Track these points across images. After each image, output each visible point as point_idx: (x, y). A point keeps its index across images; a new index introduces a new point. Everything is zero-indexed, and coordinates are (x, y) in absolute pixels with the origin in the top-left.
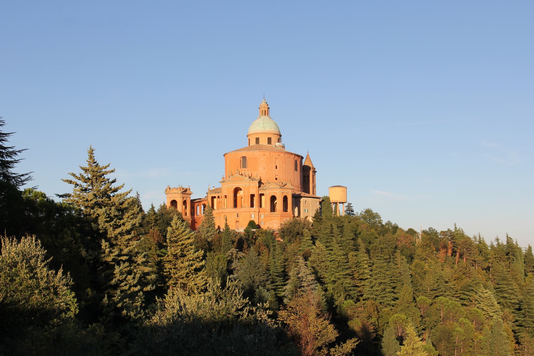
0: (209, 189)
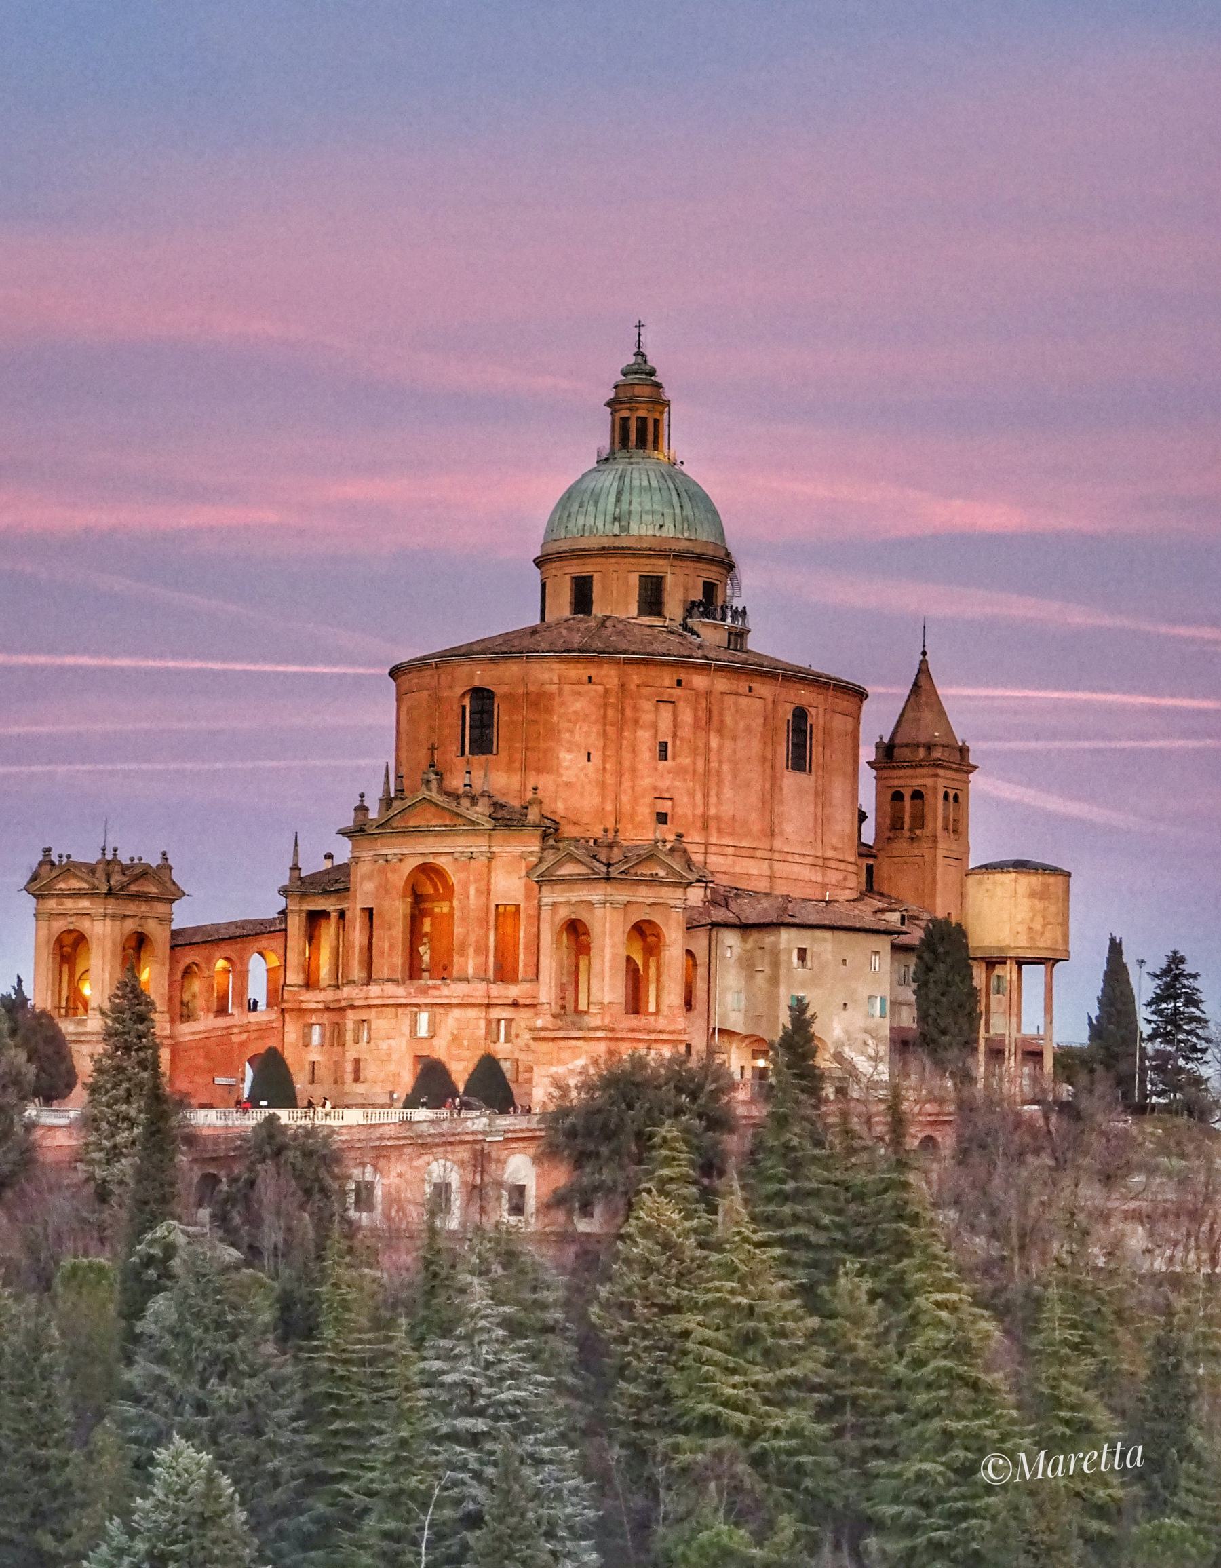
0: (295, 868)
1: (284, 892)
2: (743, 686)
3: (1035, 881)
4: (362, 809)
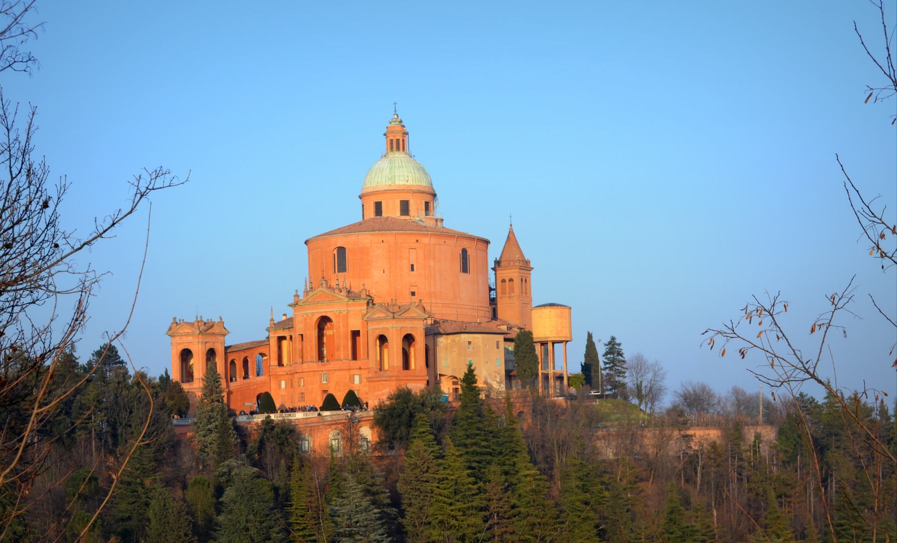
0: (272, 320)
1: (268, 330)
2: (442, 241)
4: (297, 296)
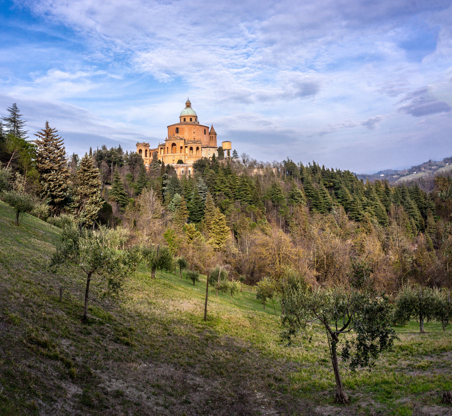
3: (229, 143)
4: (166, 138)
